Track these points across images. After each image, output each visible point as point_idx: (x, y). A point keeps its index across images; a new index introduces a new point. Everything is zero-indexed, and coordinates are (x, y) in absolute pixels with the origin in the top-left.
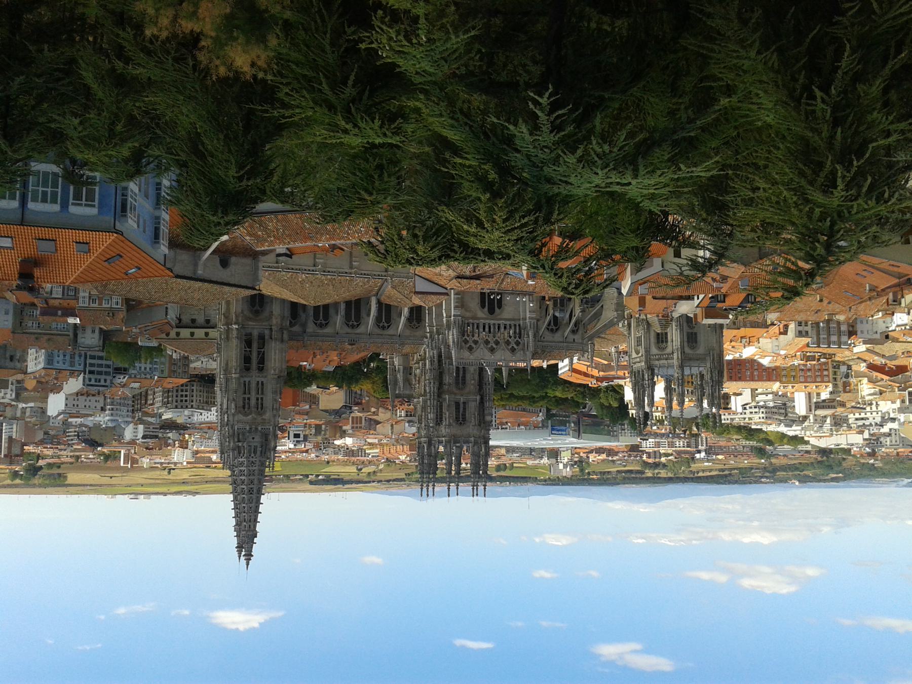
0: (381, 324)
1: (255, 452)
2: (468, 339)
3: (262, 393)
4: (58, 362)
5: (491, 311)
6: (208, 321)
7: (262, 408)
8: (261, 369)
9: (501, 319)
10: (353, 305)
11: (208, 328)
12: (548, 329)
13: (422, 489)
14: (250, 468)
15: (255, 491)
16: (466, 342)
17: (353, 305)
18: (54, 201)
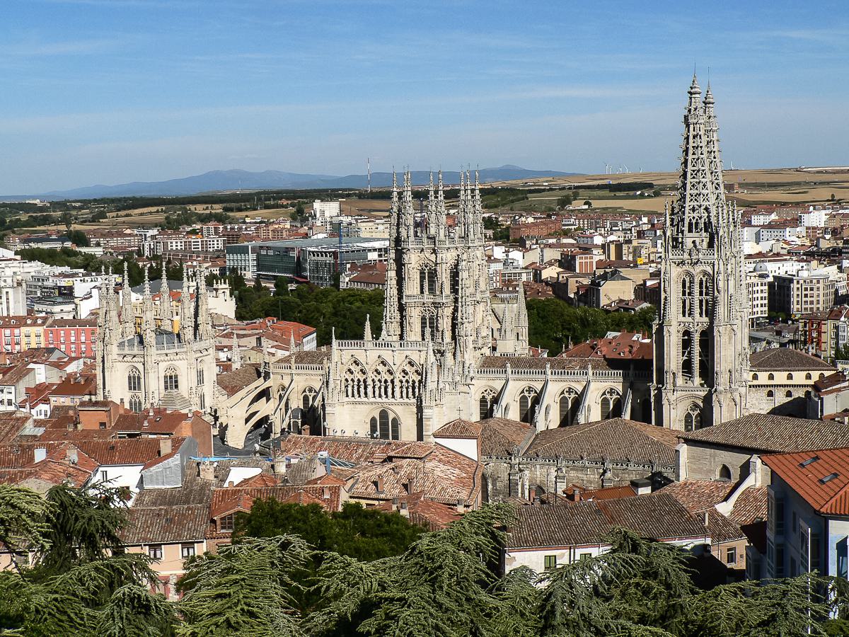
1: (690, 224)
3: (684, 302)
5: (384, 414)
6: (770, 394)
8: (687, 333)
11: (770, 386)
12: (315, 391)
14: (696, 203)
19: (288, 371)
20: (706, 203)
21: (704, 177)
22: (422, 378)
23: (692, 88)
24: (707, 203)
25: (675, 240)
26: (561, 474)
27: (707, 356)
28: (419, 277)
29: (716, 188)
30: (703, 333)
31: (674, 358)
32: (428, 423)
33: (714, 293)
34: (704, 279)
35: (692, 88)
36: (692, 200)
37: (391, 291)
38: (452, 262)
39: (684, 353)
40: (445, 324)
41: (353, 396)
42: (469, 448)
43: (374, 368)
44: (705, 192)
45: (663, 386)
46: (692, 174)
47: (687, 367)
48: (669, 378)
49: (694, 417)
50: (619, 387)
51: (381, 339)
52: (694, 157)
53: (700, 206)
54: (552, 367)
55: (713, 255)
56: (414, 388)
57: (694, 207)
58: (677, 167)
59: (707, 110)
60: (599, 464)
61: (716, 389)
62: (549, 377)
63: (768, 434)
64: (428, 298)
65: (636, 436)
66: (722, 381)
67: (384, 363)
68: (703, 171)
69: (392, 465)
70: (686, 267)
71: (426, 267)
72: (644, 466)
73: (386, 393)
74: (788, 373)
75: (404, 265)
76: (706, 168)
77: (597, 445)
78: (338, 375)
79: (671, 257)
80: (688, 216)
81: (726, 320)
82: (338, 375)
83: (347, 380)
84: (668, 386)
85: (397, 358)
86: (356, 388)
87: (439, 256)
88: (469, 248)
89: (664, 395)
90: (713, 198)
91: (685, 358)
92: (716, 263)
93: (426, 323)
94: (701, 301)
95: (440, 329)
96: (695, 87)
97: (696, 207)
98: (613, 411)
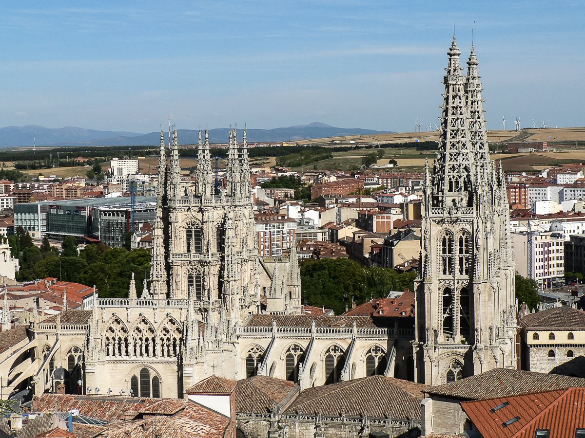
1: (451, 183)
3: (444, 260)
5: (145, 373)
6: (552, 354)
7: (444, 239)
8: (447, 290)
9: (132, 362)
11: (551, 345)
14: (455, 163)
19: (54, 331)
20: (465, 163)
21: (463, 137)
22: (183, 336)
23: (451, 49)
24: (467, 163)
25: (435, 198)
26: (319, 432)
27: (468, 313)
28: (185, 236)
29: (481, 148)
30: (463, 291)
31: (435, 316)
32: (188, 381)
33: (473, 251)
34: (464, 237)
35: (451, 49)
36: (451, 159)
37: (158, 249)
38: (220, 220)
39: (445, 310)
40: (211, 282)
41: (114, 355)
42: (222, 405)
43: (135, 326)
44: (464, 151)
45: (424, 343)
46: (451, 134)
47: (448, 324)
48: (430, 335)
49: (456, 375)
50: (384, 345)
51: (142, 297)
52: (453, 117)
53: (460, 166)
54: (318, 325)
55: (472, 213)
56: (175, 346)
57: (453, 167)
58: (438, 127)
59: (471, 70)
60: (357, 421)
61: (476, 346)
62: (315, 335)
63: (509, 388)
64: (194, 257)
65: (395, 394)
66: (482, 338)
67: (145, 321)
68: (463, 131)
69: (141, 422)
70: (447, 226)
71: (193, 225)
72: (401, 423)
73: (147, 351)
74: (568, 332)
75: (170, 223)
76: (466, 127)
77: (356, 402)
78: (99, 334)
79: (431, 215)
80: (448, 175)
81: (486, 277)
82: (99, 334)
83: (108, 339)
84: (429, 343)
85: (158, 316)
86: (117, 346)
87: (206, 214)
88: (236, 206)
89: (425, 352)
90: (471, 156)
91: (446, 315)
92: (475, 221)
93: (192, 282)
94: (461, 259)
95: (207, 288)
96: (454, 49)
97: (455, 166)
98: (377, 369)
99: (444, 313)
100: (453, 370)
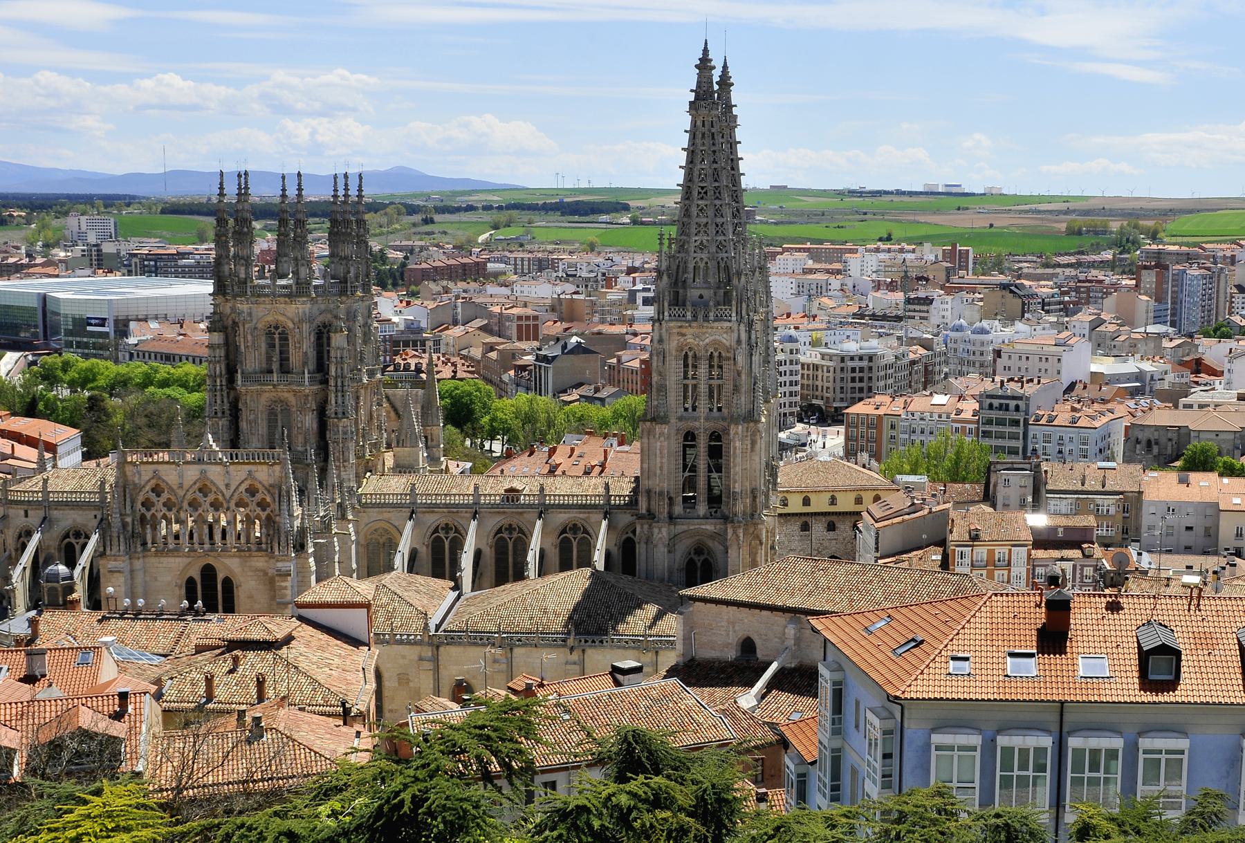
0: (452, 535)
2: (258, 510)
3: (686, 387)
4: (1071, 439)
5: (208, 573)
7: (686, 356)
10: (511, 572)
13: (360, 190)
15: (695, 194)
16: (262, 505)
17: (511, 572)
18: (1008, 752)
46: (699, 193)
49: (699, 564)
91: (687, 474)
99: (684, 471)
100: (696, 558)
